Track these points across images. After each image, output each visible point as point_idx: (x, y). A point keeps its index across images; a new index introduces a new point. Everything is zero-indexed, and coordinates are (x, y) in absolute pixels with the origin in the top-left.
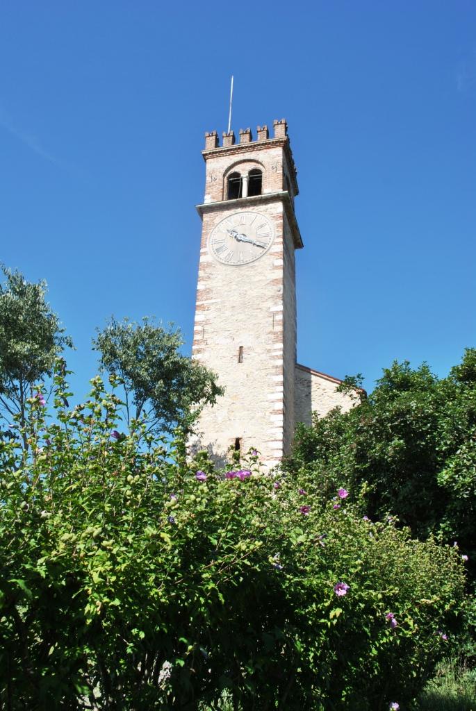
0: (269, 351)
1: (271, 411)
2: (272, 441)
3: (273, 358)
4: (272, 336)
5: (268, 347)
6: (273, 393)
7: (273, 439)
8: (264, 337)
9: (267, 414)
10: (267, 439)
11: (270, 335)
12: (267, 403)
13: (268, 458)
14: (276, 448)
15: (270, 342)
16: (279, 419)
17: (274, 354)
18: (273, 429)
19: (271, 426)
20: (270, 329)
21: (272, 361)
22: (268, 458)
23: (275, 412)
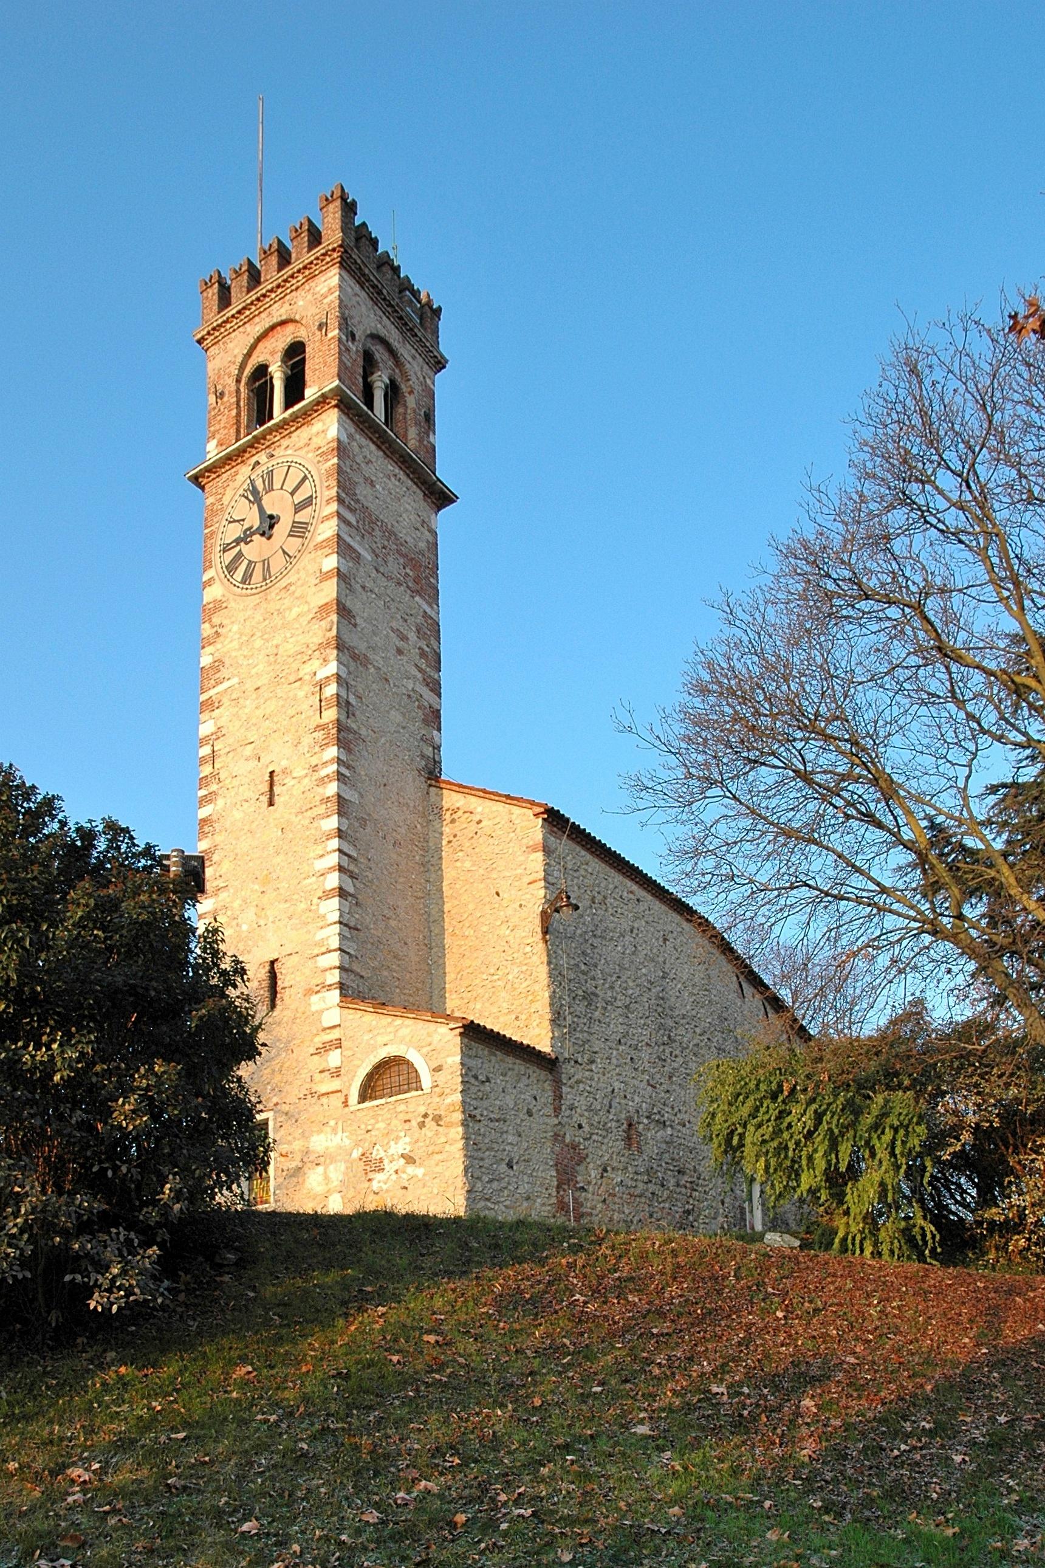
0: (315, 768)
1: (320, 894)
2: (323, 954)
3: (322, 781)
4: (319, 735)
5: (314, 761)
6: (322, 856)
7: (324, 949)
8: (307, 740)
9: (315, 901)
10: (316, 952)
11: (316, 735)
12: (314, 879)
13: (318, 988)
14: (328, 966)
15: (317, 749)
16: (332, 908)
17: (324, 772)
18: (323, 930)
19: (321, 924)
20: (316, 720)
21: (320, 790)
22: (318, 988)
23: (326, 895)
